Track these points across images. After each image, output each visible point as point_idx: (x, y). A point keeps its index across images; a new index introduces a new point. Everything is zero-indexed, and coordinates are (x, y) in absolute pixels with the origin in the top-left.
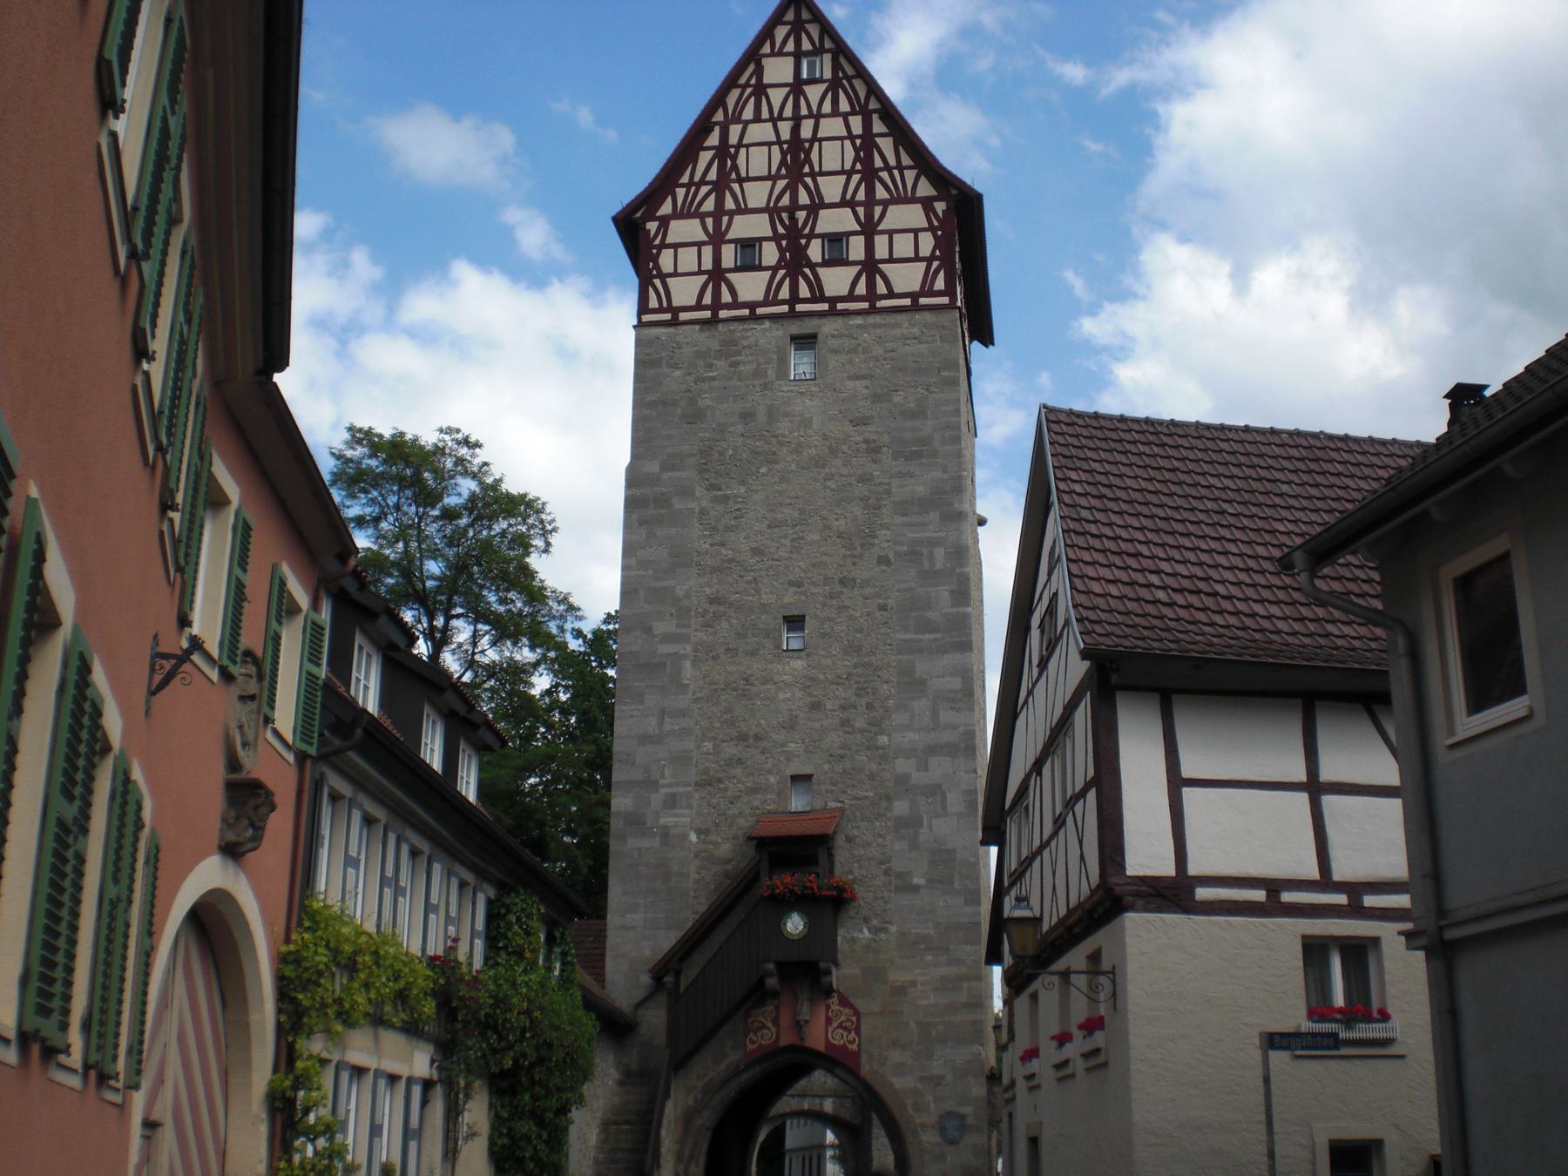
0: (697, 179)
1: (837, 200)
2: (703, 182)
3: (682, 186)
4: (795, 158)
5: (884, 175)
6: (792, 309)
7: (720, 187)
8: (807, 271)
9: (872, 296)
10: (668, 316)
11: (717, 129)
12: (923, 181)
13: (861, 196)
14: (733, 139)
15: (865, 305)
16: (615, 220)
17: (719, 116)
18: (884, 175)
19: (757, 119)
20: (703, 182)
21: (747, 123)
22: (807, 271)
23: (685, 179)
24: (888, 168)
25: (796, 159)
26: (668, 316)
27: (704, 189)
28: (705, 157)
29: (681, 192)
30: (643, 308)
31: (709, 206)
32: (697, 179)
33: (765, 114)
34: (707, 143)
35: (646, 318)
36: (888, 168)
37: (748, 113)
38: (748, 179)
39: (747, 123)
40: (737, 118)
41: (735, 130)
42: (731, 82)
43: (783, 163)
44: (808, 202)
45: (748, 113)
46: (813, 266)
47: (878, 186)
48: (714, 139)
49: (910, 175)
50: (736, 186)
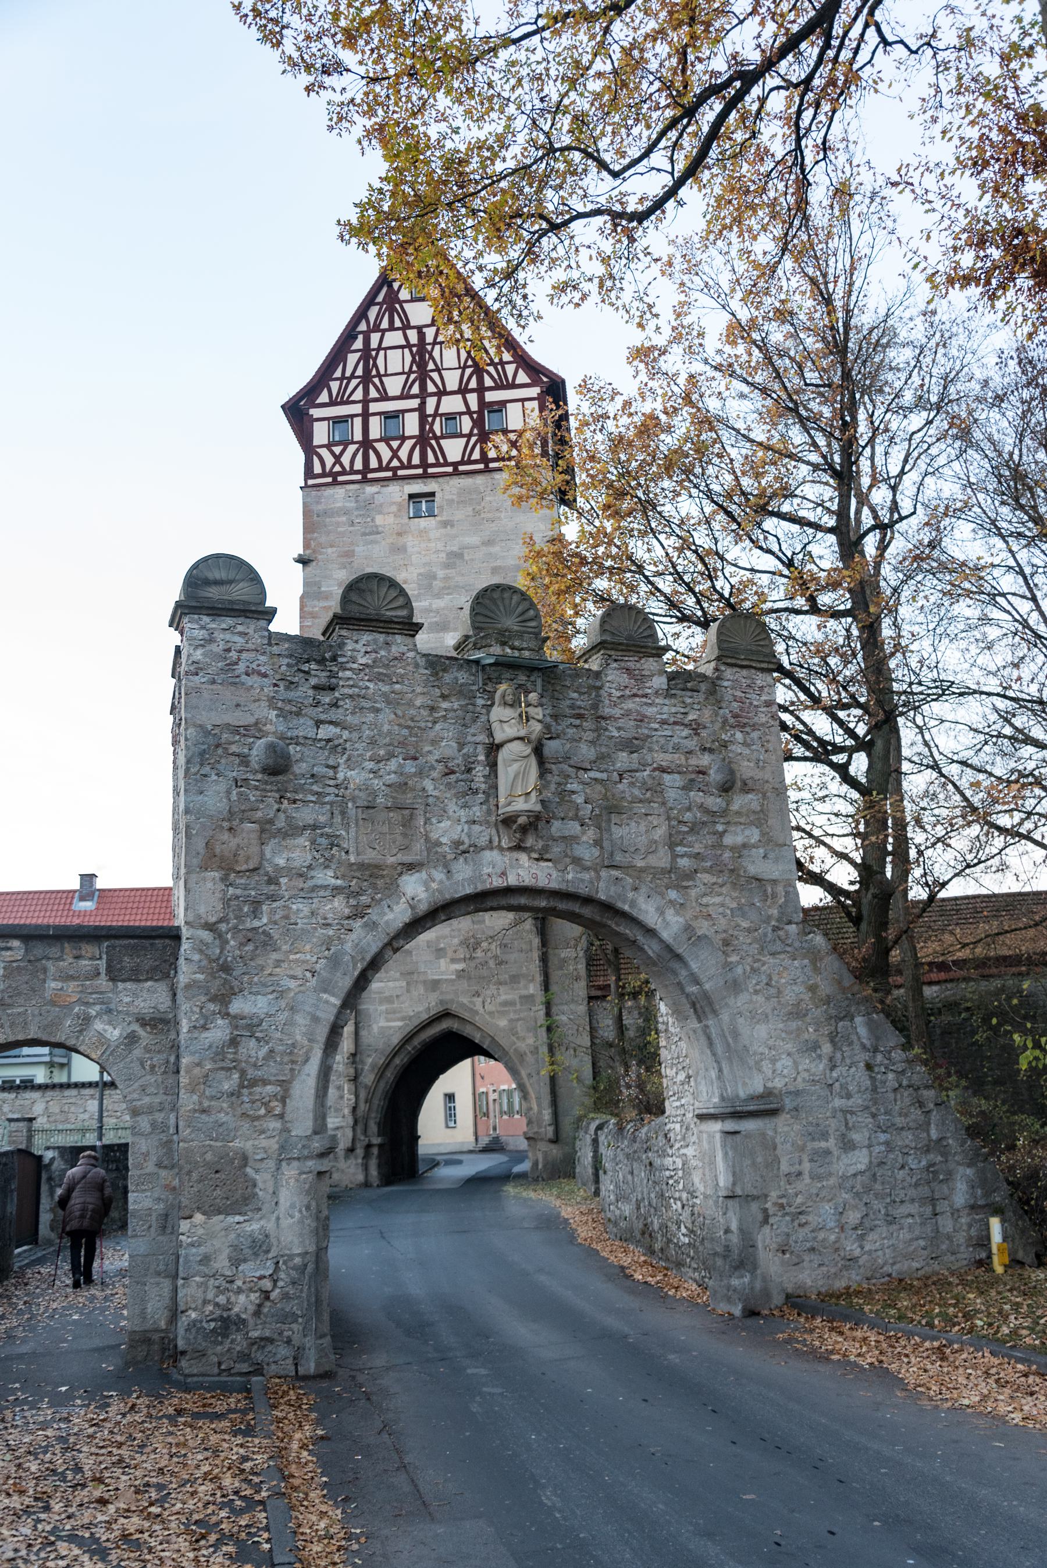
0: (348, 374)
1: (456, 388)
2: (353, 376)
3: (336, 379)
4: (422, 357)
5: (491, 369)
6: (425, 471)
7: (366, 380)
8: (433, 442)
9: (484, 459)
10: (330, 480)
11: (361, 337)
12: (521, 372)
13: (473, 384)
14: (374, 344)
15: (481, 466)
16: (283, 407)
17: (363, 327)
18: (491, 369)
19: (392, 328)
20: (353, 376)
21: (384, 331)
22: (433, 442)
23: (338, 374)
24: (492, 363)
25: (421, 356)
26: (330, 480)
27: (354, 382)
28: (352, 359)
29: (335, 386)
30: (309, 473)
31: (358, 395)
32: (348, 374)
33: (398, 323)
34: (354, 347)
35: (310, 482)
36: (492, 363)
37: (385, 324)
38: (386, 375)
39: (384, 331)
40: (377, 328)
41: (375, 338)
42: (370, 301)
43: (413, 361)
44: (435, 390)
45: (385, 324)
46: (437, 439)
47: (486, 376)
48: (358, 344)
49: (510, 369)
50: (376, 380)
